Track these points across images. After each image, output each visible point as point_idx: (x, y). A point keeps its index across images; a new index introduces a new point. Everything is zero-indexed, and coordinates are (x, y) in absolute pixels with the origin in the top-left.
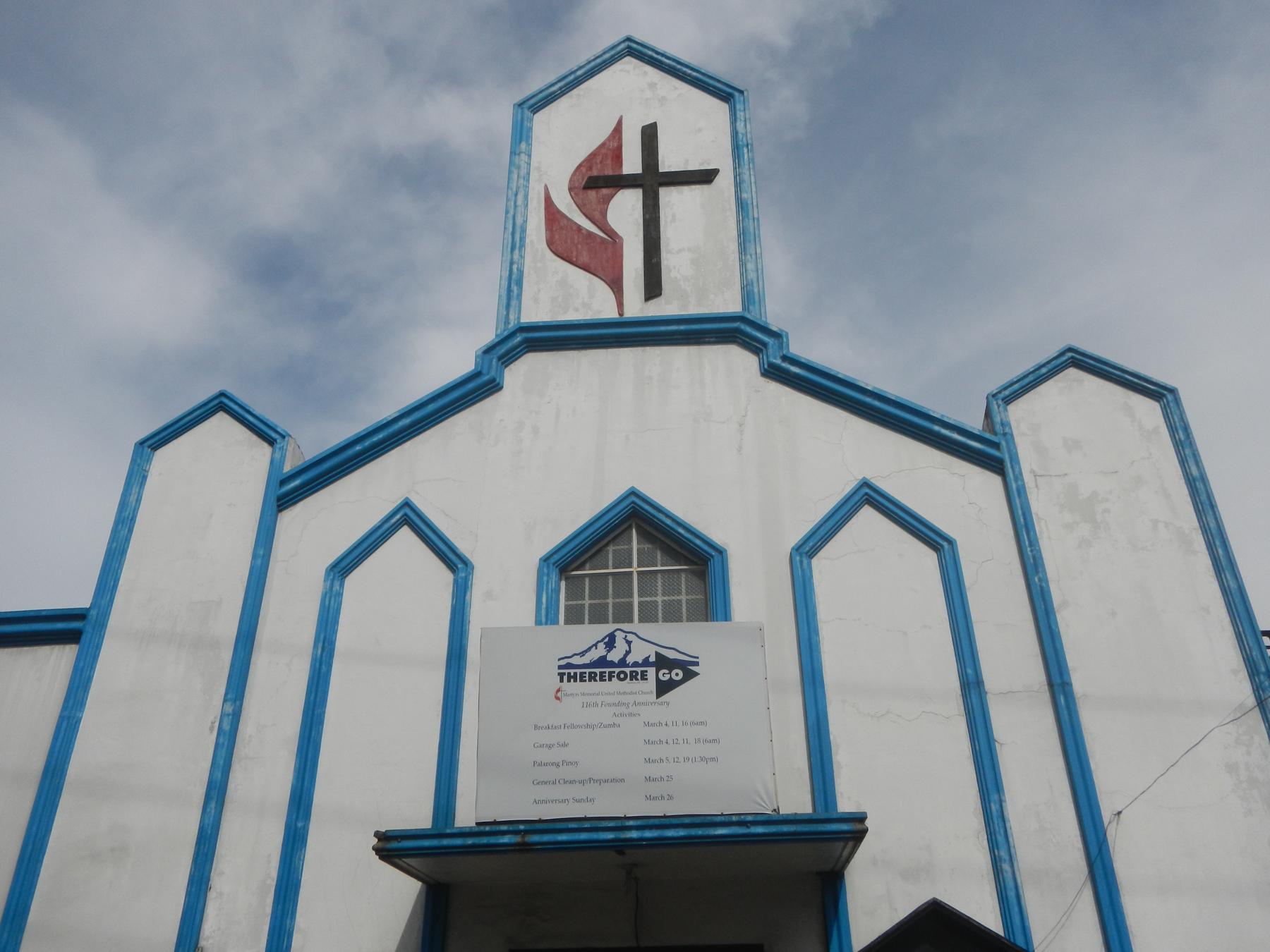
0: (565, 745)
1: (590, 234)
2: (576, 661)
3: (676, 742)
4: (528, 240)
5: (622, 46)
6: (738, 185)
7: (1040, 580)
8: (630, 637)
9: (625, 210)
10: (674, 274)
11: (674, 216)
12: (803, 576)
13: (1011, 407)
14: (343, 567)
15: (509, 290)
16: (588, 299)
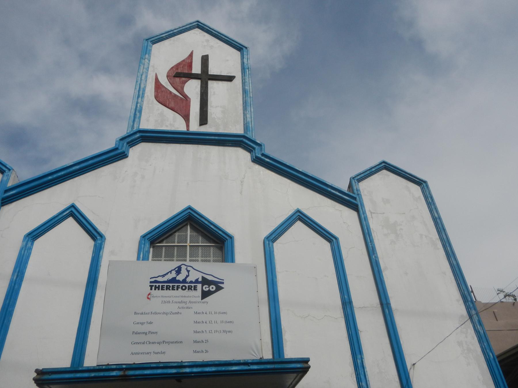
0: (151, 323)
1: (175, 95)
2: (160, 279)
3: (211, 322)
4: (146, 95)
5: (195, 24)
6: (244, 83)
8: (189, 268)
9: (192, 89)
10: (213, 116)
11: (214, 92)
12: (270, 251)
14: (35, 235)
15: (135, 114)
16: (174, 122)
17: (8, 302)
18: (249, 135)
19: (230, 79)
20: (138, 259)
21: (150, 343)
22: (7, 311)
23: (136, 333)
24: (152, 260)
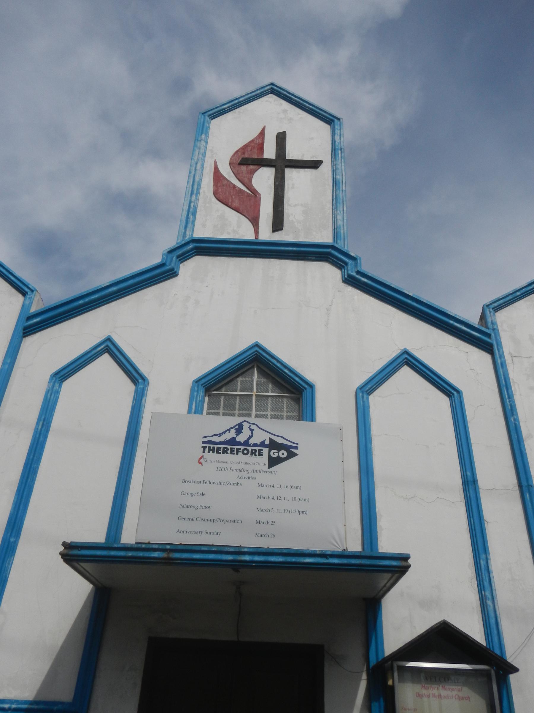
0: (203, 495)
1: (241, 190)
2: (215, 439)
3: (279, 498)
4: (201, 191)
5: (268, 87)
6: (334, 171)
7: (514, 419)
8: (253, 427)
9: (263, 180)
10: (291, 218)
11: (293, 185)
12: (364, 406)
13: (498, 314)
14: (63, 375)
15: (187, 218)
16: (238, 228)
17: (31, 457)
18: (339, 245)
19: (315, 165)
20: (189, 412)
21: (201, 520)
22: (31, 467)
23: (184, 506)
24: (208, 414)
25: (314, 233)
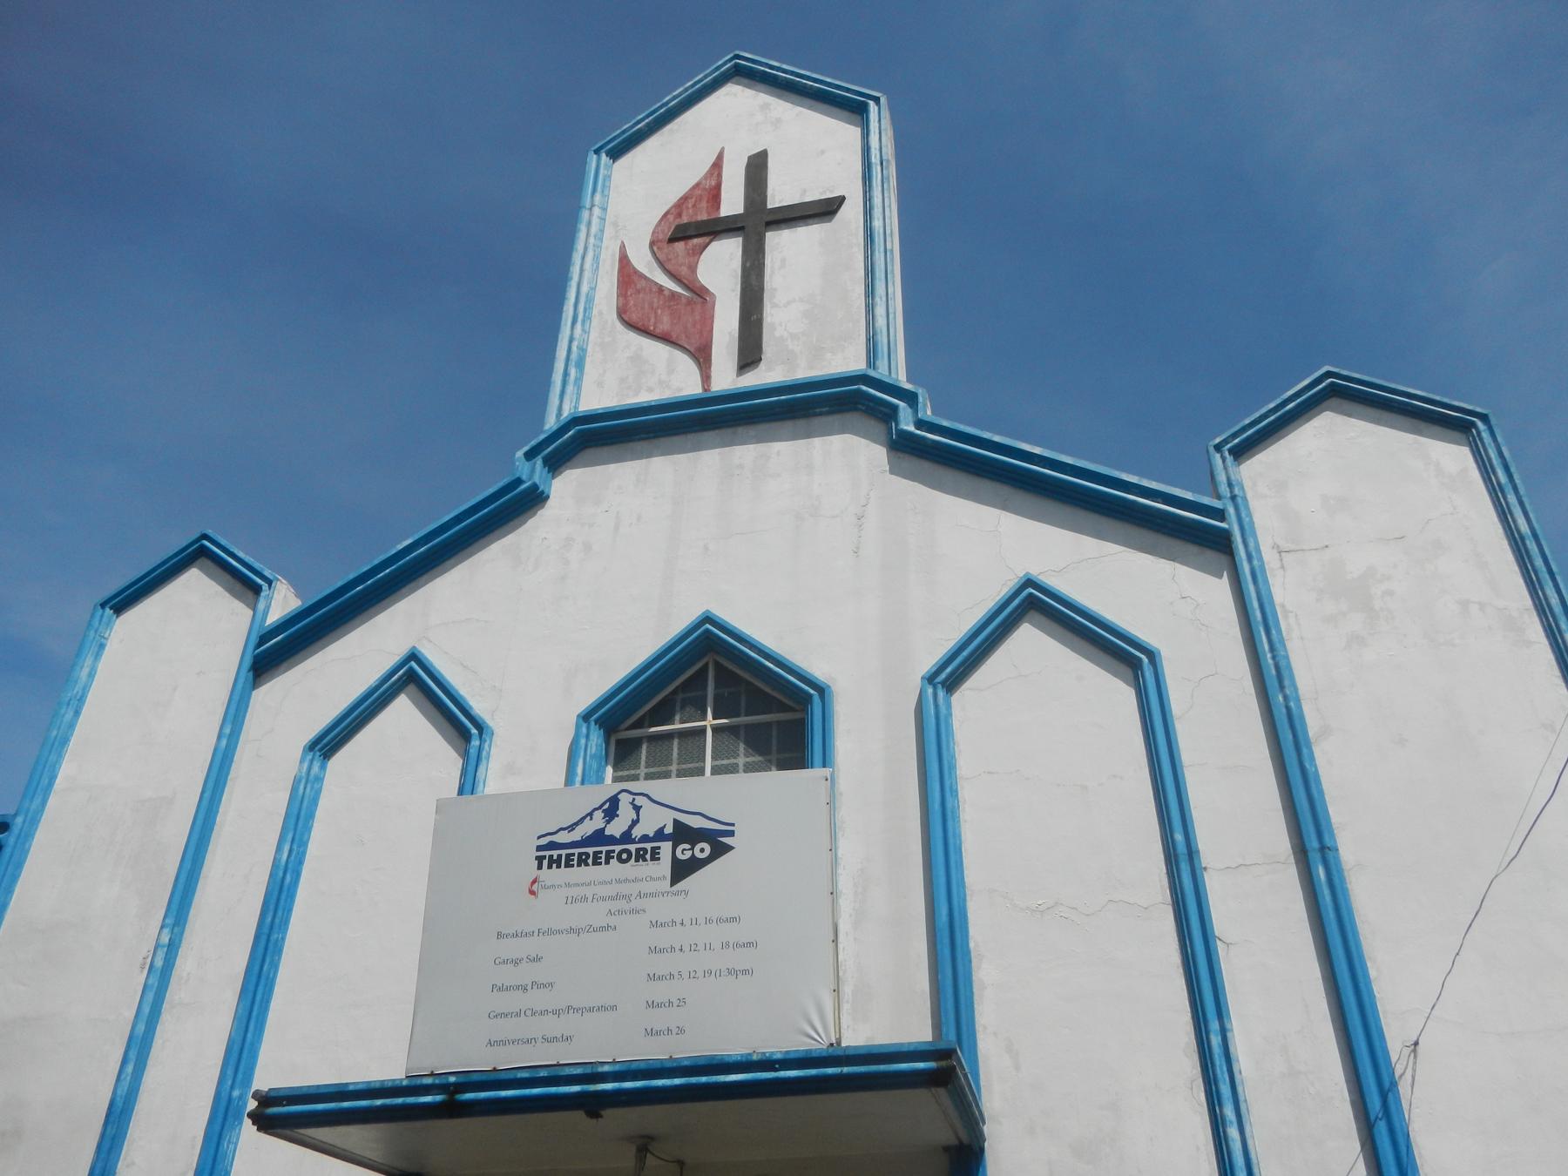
0: (538, 959)
1: (673, 295)
3: (694, 948)
4: (595, 312)
8: (640, 801)
11: (783, 261)
14: (329, 743)
16: (667, 376)
17: (269, 920)
18: (881, 372)
19: (826, 209)
20: (569, 781)
21: (533, 1014)
22: (268, 940)
24: (616, 780)
25: (829, 355)
